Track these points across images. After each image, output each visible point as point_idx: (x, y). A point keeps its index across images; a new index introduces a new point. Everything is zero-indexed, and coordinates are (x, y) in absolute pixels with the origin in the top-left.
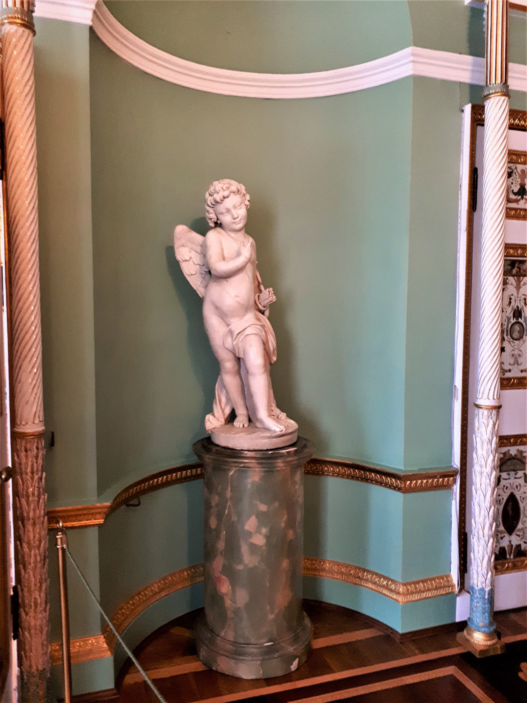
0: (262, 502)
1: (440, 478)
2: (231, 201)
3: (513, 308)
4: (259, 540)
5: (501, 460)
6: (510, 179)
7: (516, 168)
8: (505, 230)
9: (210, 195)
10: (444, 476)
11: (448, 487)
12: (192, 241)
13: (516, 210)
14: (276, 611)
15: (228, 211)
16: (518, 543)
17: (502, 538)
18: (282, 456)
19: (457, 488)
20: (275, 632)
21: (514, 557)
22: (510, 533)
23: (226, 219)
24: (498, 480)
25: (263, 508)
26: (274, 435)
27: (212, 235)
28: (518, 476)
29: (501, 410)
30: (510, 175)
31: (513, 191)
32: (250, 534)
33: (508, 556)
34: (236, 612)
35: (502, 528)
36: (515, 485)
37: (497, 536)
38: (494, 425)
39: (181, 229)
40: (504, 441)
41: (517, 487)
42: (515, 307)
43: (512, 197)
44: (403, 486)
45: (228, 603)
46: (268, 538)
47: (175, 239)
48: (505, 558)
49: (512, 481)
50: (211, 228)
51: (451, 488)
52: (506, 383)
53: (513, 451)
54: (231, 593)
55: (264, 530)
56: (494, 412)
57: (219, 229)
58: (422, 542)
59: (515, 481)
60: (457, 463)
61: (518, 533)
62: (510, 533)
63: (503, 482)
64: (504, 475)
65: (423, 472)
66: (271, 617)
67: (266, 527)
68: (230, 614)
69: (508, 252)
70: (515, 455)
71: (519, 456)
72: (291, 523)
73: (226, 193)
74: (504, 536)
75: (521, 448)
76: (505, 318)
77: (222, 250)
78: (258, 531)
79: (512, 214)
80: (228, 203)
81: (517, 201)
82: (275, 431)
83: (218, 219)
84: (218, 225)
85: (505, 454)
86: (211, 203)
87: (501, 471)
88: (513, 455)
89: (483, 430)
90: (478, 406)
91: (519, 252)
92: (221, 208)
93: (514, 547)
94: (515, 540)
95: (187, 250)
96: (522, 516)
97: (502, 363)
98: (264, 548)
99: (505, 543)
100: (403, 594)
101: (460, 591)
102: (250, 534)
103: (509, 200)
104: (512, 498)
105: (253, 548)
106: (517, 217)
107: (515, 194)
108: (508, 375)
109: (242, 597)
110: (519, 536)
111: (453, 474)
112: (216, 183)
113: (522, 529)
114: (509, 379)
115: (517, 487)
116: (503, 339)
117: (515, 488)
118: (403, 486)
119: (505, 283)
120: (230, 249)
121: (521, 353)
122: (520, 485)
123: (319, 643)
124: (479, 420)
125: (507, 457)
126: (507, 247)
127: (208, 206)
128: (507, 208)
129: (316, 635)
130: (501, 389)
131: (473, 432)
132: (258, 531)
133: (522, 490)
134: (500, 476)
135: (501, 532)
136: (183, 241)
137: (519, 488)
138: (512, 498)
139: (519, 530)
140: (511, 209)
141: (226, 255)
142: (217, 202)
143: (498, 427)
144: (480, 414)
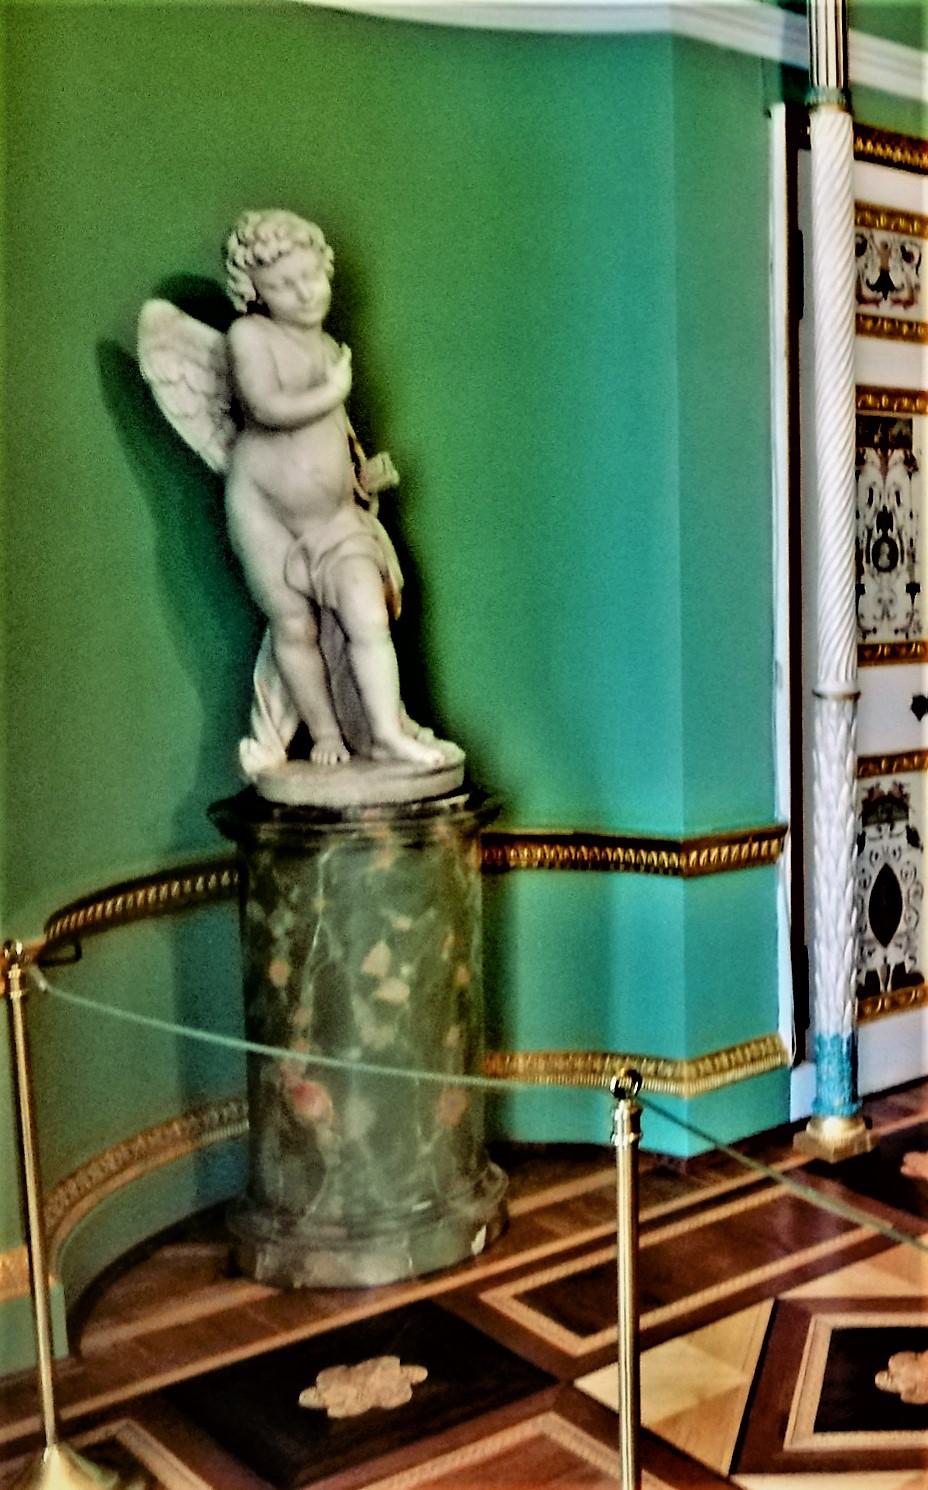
0: (400, 910)
1: (754, 841)
2: (295, 261)
3: (876, 509)
4: (396, 991)
5: (865, 803)
6: (863, 258)
7: (872, 237)
8: (855, 360)
9: (240, 242)
10: (761, 836)
11: (769, 860)
12: (189, 341)
13: (875, 319)
14: (436, 1136)
15: (289, 283)
16: (899, 961)
17: (870, 954)
18: (438, 812)
19: (785, 860)
20: (434, 1177)
21: (893, 988)
22: (885, 943)
23: (282, 299)
24: (860, 840)
25: (403, 923)
26: (421, 769)
27: (247, 334)
28: (895, 831)
29: (859, 701)
30: (861, 249)
31: (868, 282)
32: (371, 983)
33: (882, 987)
34: (348, 1153)
35: (870, 934)
36: (891, 851)
37: (863, 954)
38: (849, 728)
39: (158, 311)
40: (866, 766)
41: (895, 853)
42: (881, 509)
43: (867, 292)
44: (683, 862)
45: (325, 1136)
46: (417, 985)
47: (140, 331)
48: (877, 992)
49: (886, 841)
50: (239, 315)
51: (774, 863)
52: (867, 655)
53: (886, 784)
54: (332, 1112)
55: (406, 970)
56: (849, 704)
57: (259, 319)
58: (722, 970)
59: (887, 841)
60: (784, 812)
61: (899, 941)
62: (885, 943)
63: (868, 846)
64: (871, 831)
65: (724, 833)
66: (426, 1149)
67: (410, 960)
68: (331, 1160)
69: (864, 403)
70: (890, 794)
71: (897, 796)
72: (460, 956)
73: (285, 245)
74: (874, 950)
75: (902, 778)
76: (862, 528)
77: (275, 366)
78: (393, 971)
79: (865, 326)
80: (291, 266)
81: (876, 302)
82: (422, 763)
83: (258, 295)
84: (260, 308)
85: (871, 791)
86: (246, 262)
87: (865, 823)
88: (886, 791)
89: (830, 738)
90: (819, 696)
91: (884, 400)
92: (271, 275)
93: (892, 968)
94: (894, 955)
95: (175, 359)
96: (904, 908)
97: (859, 616)
98: (407, 1006)
99: (876, 963)
100: (690, 1079)
101: (797, 1063)
102: (371, 983)
103: (860, 299)
104: (887, 874)
105: (384, 1011)
106: (877, 332)
107: (872, 288)
108: (871, 639)
109: (360, 1116)
110: (901, 946)
111: (778, 833)
112: (254, 217)
113: (906, 933)
114: (874, 647)
115: (895, 853)
116: (859, 571)
117: (892, 856)
118: (683, 862)
119: (860, 461)
120: (294, 364)
121: (893, 597)
122: (900, 849)
123: (520, 1207)
124: (822, 722)
125: (876, 795)
126: (861, 391)
127: (235, 264)
128: (858, 316)
129: (513, 1194)
130: (859, 665)
131: (813, 745)
132: (393, 971)
133: (904, 859)
134: (864, 834)
135: (870, 942)
136: (163, 337)
137: (898, 853)
138: (887, 874)
139: (900, 936)
140: (866, 317)
141: (285, 376)
142: (260, 262)
143: (856, 734)
144: (824, 709)
